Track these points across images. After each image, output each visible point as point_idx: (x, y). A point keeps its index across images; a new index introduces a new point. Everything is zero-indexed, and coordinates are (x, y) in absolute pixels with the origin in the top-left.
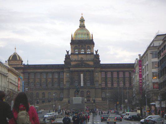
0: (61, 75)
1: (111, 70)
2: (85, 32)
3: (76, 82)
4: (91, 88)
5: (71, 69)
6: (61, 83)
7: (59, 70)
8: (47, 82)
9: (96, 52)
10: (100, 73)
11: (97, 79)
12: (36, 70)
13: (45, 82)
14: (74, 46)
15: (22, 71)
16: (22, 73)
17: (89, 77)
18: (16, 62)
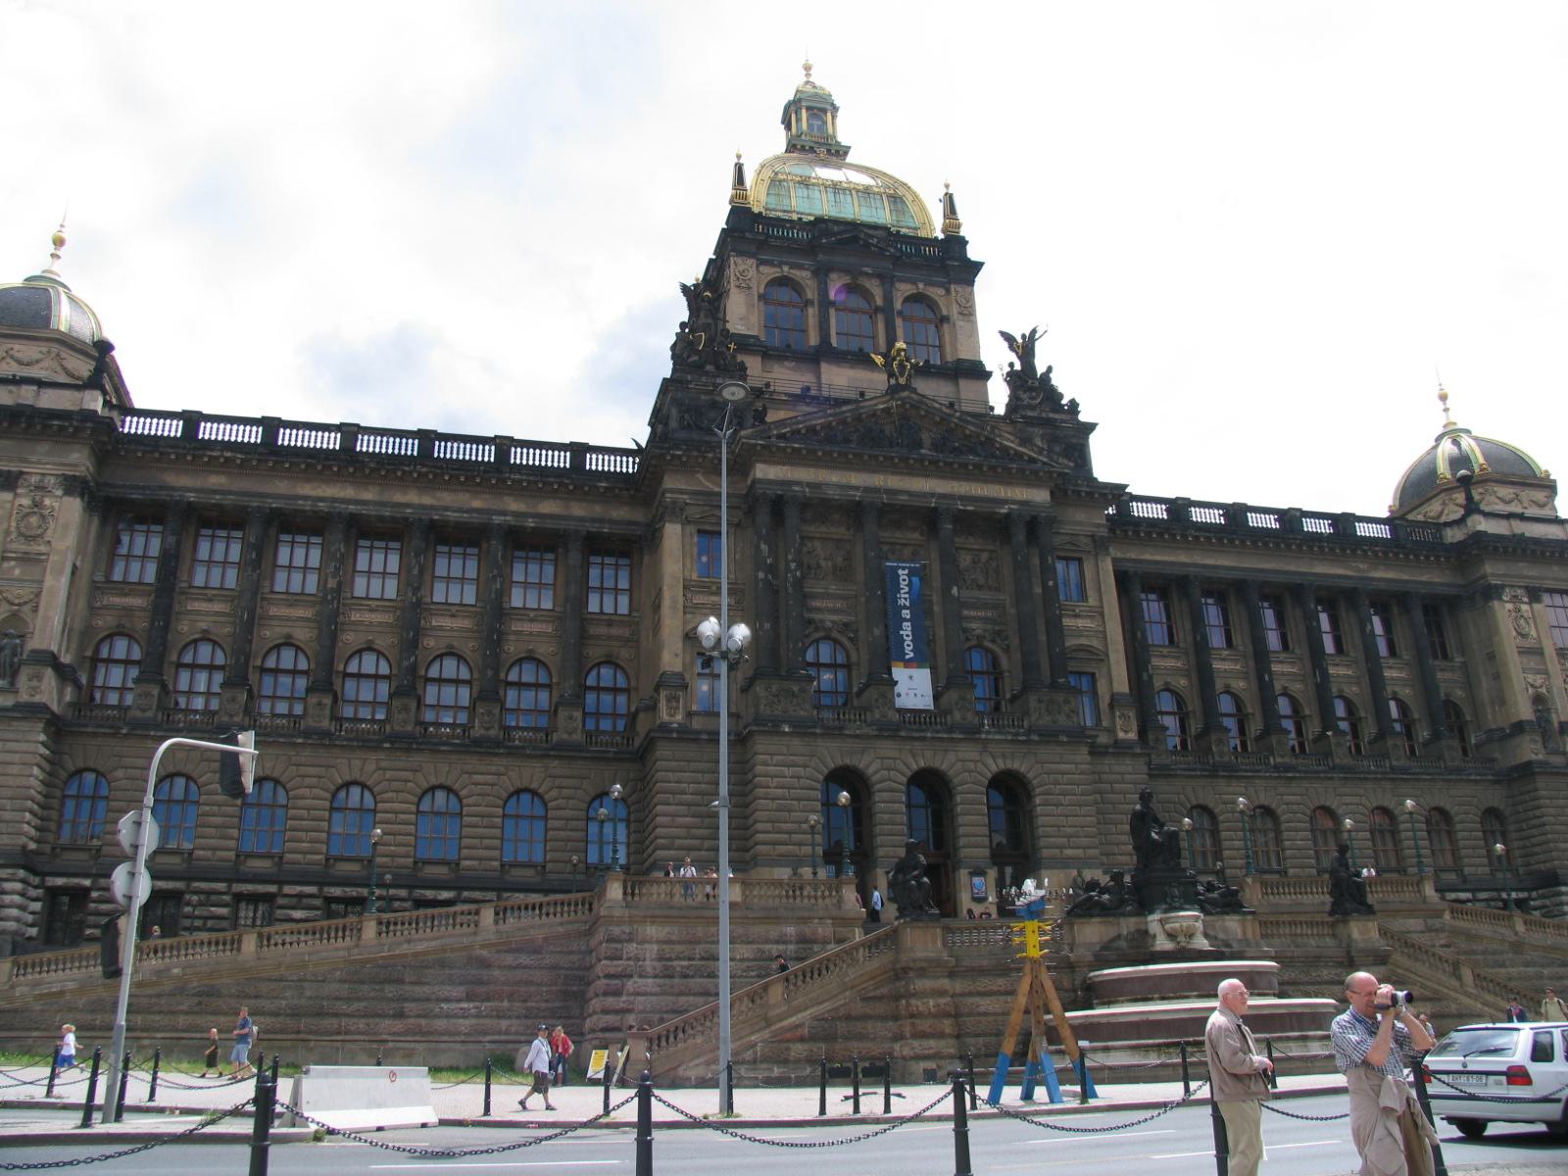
0: (594, 573)
1: (1182, 557)
2: (864, 180)
3: (825, 652)
4: (1049, 736)
5: (764, 471)
6: (591, 681)
7: (578, 510)
8: (411, 645)
9: (1025, 348)
10: (1107, 566)
11: (1078, 632)
12: (281, 486)
13: (381, 643)
14: (770, 272)
15: (79, 460)
16: (72, 485)
17: (984, 595)
18: (25, 350)
